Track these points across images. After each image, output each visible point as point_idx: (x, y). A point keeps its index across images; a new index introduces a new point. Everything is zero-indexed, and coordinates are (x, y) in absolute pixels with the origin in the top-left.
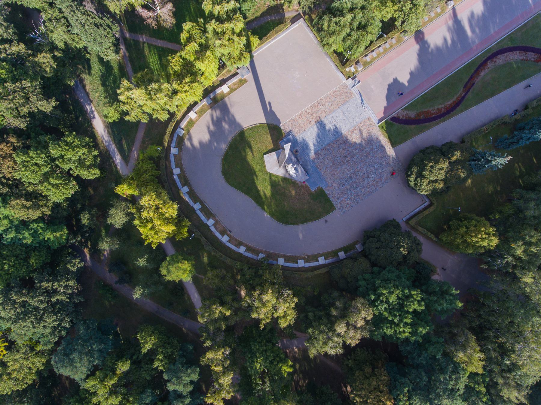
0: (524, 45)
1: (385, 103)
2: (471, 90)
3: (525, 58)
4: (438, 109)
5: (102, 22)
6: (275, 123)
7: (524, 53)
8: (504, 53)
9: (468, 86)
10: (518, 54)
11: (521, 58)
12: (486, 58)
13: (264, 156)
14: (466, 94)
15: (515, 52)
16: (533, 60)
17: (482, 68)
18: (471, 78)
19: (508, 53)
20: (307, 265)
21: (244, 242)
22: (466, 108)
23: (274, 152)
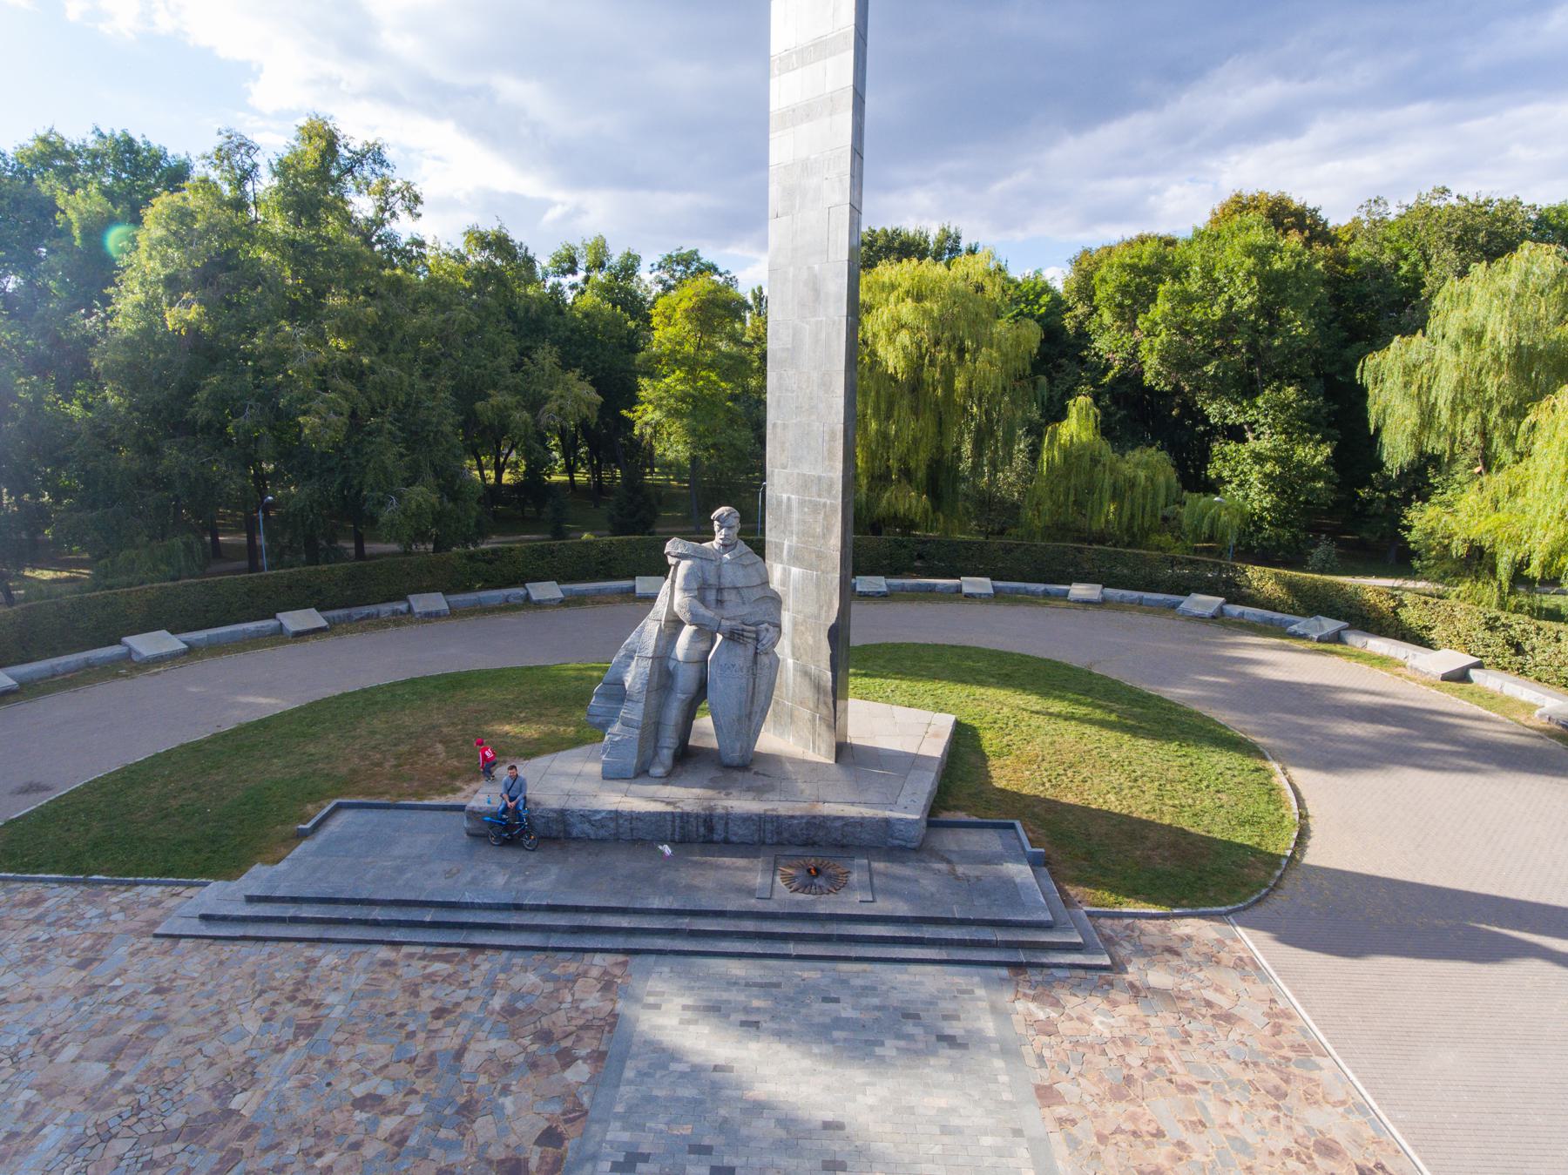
6: (1278, 901)
13: (945, 722)
21: (565, 611)
23: (935, 748)
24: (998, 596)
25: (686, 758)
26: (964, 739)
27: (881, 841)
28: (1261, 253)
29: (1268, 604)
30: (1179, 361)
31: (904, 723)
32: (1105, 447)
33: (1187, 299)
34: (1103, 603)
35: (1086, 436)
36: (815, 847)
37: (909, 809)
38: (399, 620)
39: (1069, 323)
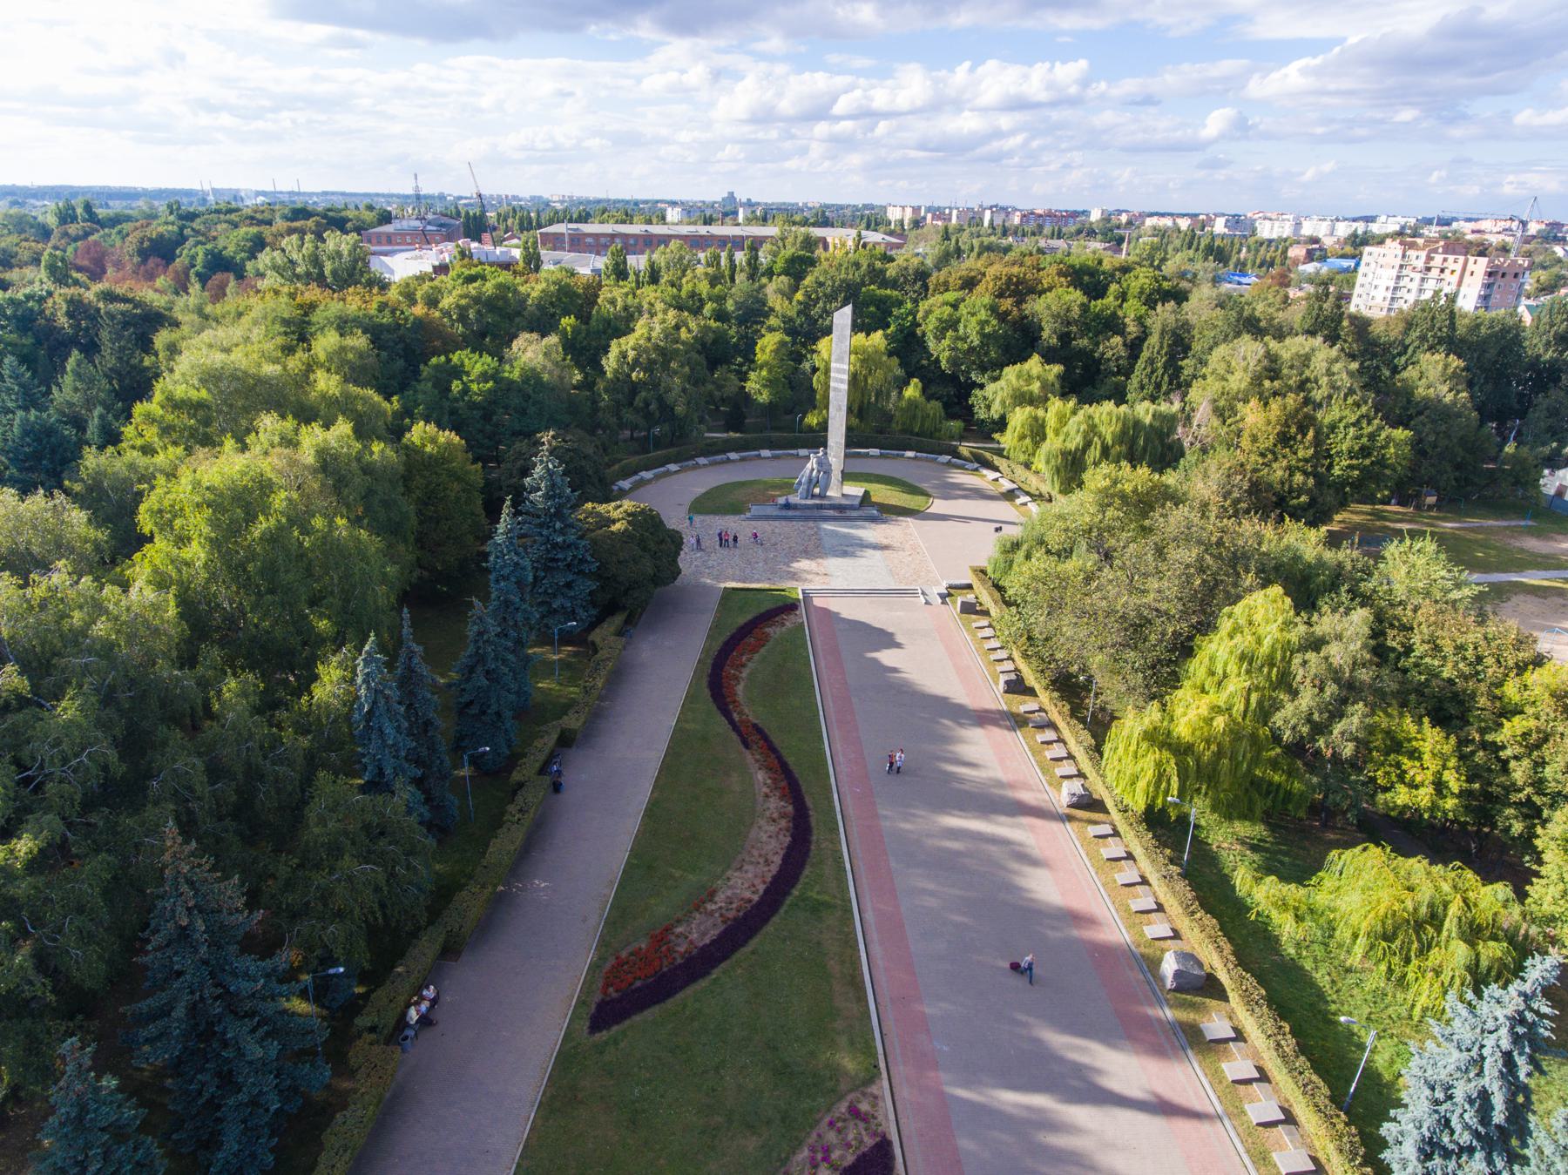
0: (769, 928)
1: (844, 615)
2: (734, 736)
3: (710, 907)
4: (743, 666)
5: (1160, 371)
7: (731, 915)
8: (785, 859)
9: (753, 736)
10: (747, 894)
11: (720, 897)
12: (809, 802)
14: (732, 722)
15: (761, 888)
16: (679, 930)
17: (783, 784)
18: (773, 749)
19: (774, 869)
20: (636, 478)
22: (691, 698)
24: (881, 456)
25: (813, 496)
26: (867, 493)
27: (852, 508)
28: (983, 324)
29: (965, 459)
30: (954, 362)
31: (855, 490)
32: (923, 399)
33: (958, 338)
34: (916, 458)
35: (917, 394)
36: (840, 508)
37: (857, 502)
38: (697, 466)
39: (919, 331)
